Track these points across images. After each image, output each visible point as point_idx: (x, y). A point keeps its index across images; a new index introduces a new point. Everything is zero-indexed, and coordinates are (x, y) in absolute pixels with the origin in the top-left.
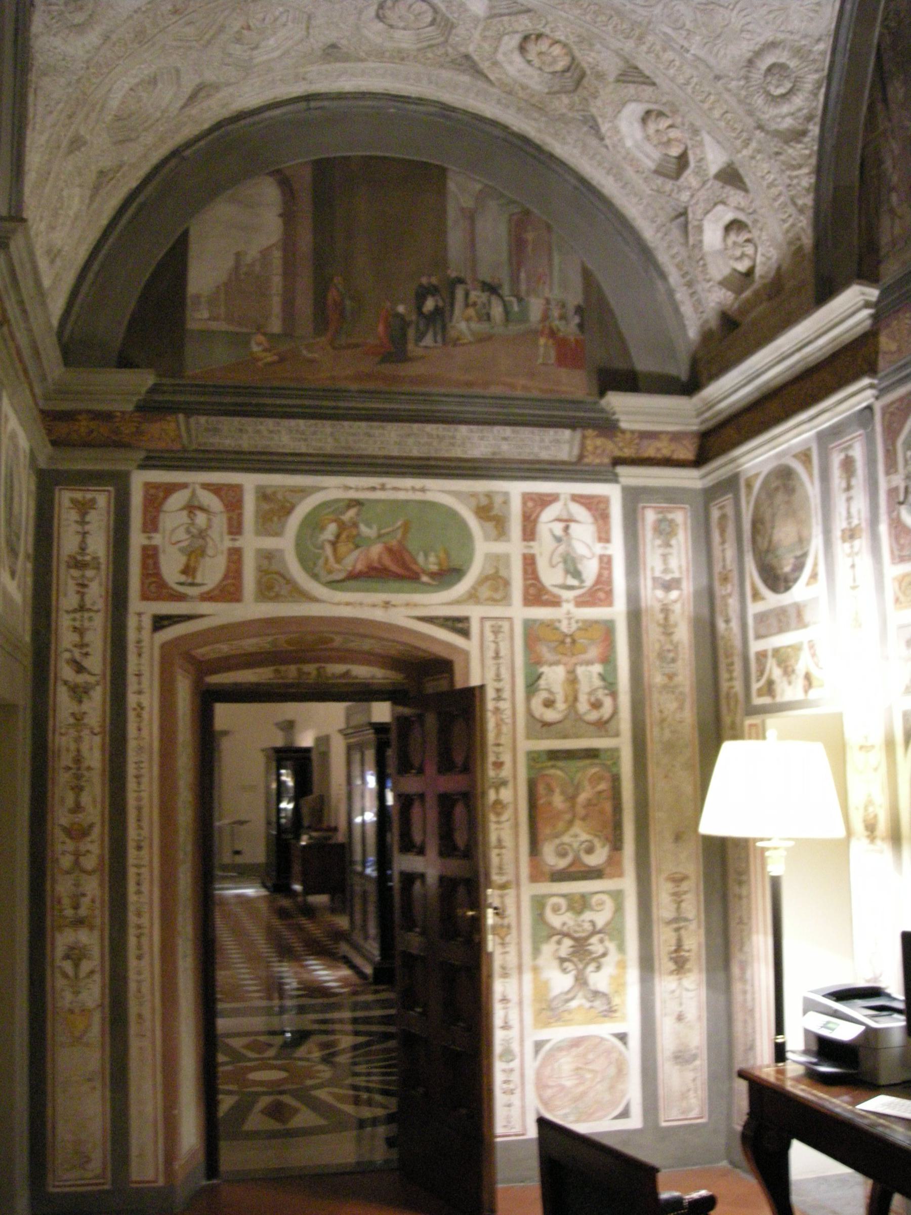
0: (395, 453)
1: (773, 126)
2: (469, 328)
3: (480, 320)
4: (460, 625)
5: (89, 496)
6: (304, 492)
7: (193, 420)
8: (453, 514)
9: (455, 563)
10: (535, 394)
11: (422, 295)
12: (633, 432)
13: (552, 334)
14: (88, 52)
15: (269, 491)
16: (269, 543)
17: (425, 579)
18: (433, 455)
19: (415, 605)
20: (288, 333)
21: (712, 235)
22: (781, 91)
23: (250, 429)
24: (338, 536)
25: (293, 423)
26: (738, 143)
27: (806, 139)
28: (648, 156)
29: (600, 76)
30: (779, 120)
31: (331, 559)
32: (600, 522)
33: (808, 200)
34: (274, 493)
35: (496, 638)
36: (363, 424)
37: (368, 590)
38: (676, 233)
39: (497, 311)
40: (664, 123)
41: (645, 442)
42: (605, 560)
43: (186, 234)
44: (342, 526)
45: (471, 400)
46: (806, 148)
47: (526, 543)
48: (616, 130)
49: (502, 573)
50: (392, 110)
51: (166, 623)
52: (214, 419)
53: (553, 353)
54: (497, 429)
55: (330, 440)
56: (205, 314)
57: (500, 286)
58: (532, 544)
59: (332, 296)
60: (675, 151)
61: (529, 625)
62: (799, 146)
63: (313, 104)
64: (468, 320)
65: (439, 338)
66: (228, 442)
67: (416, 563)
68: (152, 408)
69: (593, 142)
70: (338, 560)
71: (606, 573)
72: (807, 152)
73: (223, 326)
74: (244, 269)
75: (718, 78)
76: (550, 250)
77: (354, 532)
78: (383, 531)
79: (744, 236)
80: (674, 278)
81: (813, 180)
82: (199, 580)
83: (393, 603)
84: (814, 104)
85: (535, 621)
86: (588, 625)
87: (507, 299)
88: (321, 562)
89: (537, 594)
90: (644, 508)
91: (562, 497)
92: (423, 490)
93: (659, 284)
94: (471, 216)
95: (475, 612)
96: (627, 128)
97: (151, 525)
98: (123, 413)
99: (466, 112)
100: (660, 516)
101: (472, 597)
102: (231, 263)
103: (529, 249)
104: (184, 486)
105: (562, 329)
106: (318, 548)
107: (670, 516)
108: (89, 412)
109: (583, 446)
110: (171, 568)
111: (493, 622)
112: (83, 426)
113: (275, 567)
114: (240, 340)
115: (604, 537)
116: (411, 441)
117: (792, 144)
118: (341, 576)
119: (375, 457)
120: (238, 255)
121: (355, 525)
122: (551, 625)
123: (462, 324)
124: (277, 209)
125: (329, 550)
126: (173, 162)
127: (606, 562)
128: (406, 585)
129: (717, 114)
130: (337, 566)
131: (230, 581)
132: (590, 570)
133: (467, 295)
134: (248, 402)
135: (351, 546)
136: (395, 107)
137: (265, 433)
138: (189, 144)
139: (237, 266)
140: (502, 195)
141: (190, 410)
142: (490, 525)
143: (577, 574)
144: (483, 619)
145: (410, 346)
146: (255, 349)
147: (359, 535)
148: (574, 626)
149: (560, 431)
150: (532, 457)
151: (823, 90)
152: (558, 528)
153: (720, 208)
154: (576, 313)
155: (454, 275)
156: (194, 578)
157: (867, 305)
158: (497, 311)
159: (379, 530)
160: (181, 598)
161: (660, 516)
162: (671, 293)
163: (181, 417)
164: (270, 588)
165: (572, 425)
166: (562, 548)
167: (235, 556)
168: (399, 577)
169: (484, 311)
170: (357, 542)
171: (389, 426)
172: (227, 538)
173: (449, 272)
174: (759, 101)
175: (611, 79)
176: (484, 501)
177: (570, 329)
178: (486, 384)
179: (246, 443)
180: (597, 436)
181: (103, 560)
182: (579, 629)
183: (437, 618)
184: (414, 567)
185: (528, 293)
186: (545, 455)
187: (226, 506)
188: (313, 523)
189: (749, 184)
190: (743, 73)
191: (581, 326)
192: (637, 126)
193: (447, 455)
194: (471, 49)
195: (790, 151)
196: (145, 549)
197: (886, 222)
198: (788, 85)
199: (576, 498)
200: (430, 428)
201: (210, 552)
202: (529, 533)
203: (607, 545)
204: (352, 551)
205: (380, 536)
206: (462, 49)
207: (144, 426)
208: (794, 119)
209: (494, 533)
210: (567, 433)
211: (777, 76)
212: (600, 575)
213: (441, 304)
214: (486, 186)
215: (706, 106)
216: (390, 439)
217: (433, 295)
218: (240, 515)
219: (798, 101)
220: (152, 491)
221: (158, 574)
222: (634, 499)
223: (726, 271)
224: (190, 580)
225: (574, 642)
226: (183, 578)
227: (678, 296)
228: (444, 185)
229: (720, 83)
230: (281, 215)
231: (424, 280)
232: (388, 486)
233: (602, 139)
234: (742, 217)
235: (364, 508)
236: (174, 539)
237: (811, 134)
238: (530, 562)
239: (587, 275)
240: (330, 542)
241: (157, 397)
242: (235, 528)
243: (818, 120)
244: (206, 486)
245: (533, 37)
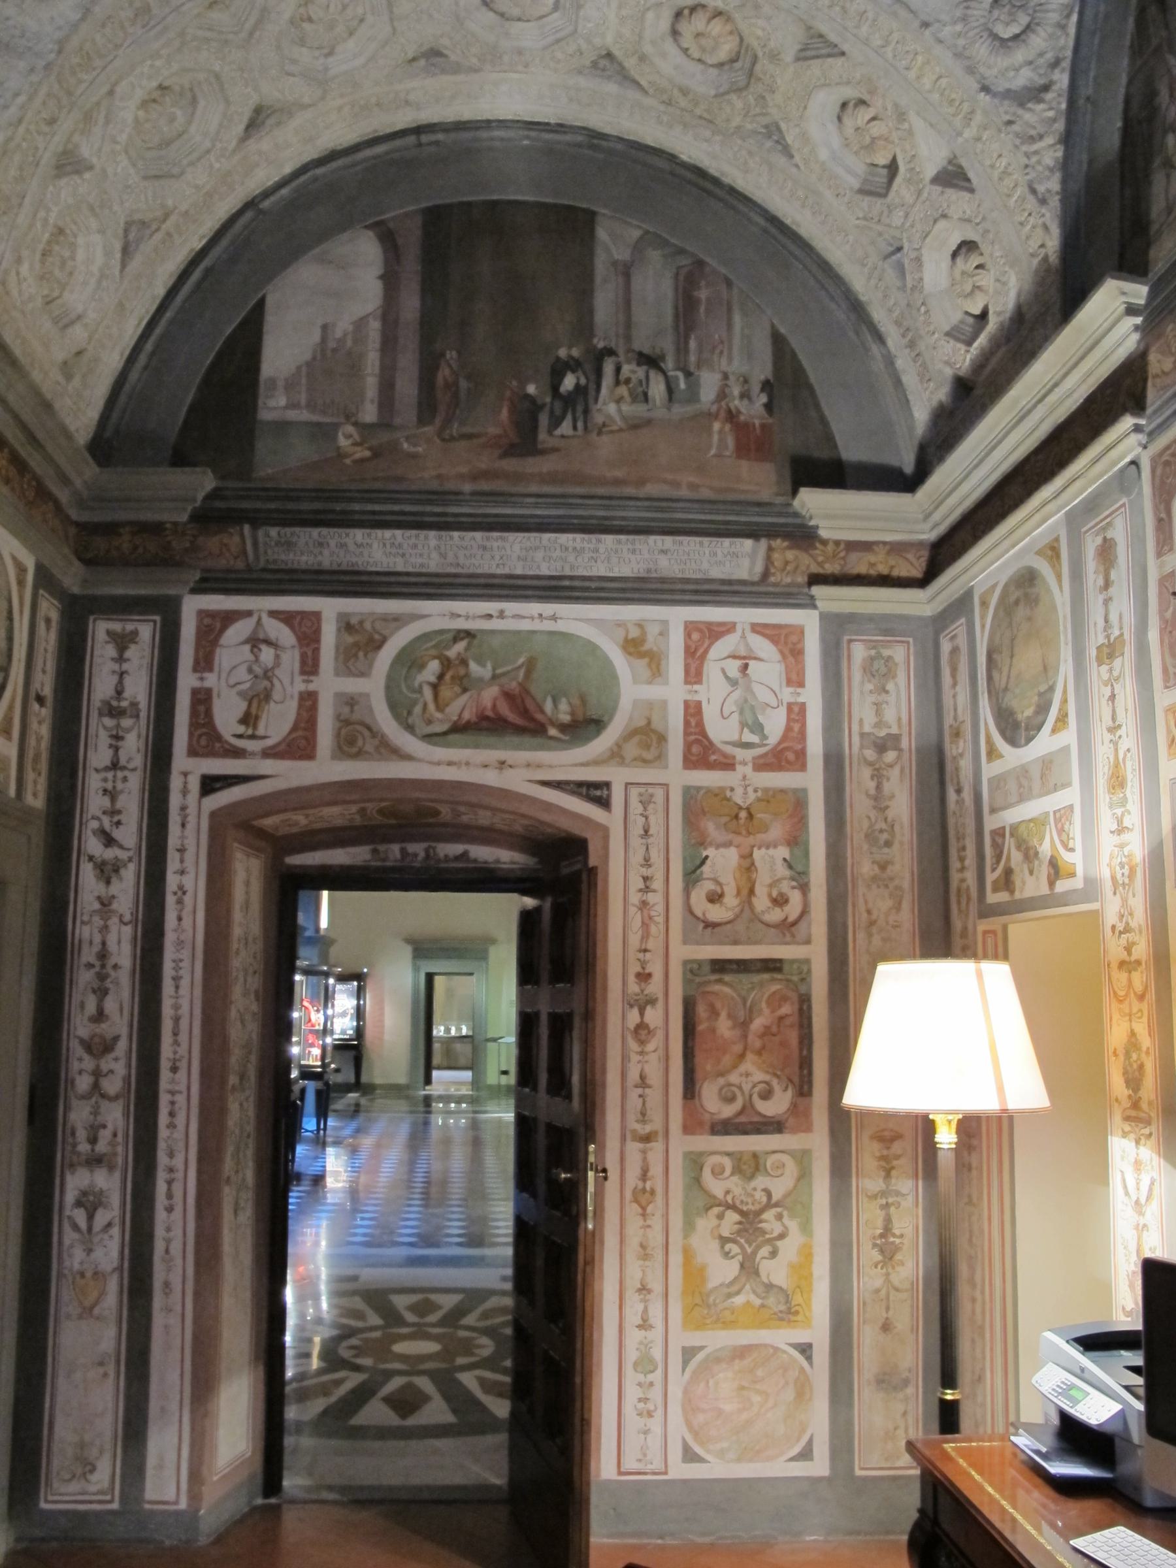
0: (519, 571)
1: (1002, 85)
2: (620, 411)
3: (634, 399)
4: (598, 793)
5: (130, 627)
6: (399, 621)
7: (261, 533)
8: (592, 648)
9: (593, 713)
10: (706, 493)
11: (558, 370)
12: (837, 543)
13: (731, 416)
14: (60, 28)
15: (354, 621)
16: (352, 685)
17: (552, 732)
18: (568, 572)
19: (539, 766)
20: (385, 423)
21: (936, 271)
22: (1015, 29)
23: (332, 543)
24: (441, 677)
25: (388, 533)
26: (958, 122)
27: (1049, 96)
29: (774, 57)
30: (1012, 74)
31: (431, 707)
32: (791, 659)
33: (1053, 184)
34: (361, 623)
35: (645, 809)
36: (478, 535)
37: (477, 747)
38: (891, 275)
39: (657, 389)
40: (864, 115)
41: (854, 556)
42: (796, 709)
43: (261, 303)
44: (446, 664)
45: (621, 503)
46: (1051, 109)
47: (689, 687)
48: (805, 137)
49: (656, 724)
50: (526, 142)
51: (218, 785)
52: (288, 530)
53: (730, 442)
54: (652, 539)
55: (434, 555)
56: (282, 401)
57: (662, 358)
58: (696, 687)
59: (444, 374)
60: (882, 159)
61: (690, 795)
62: (1042, 106)
63: (425, 138)
64: (619, 401)
65: (580, 424)
66: (304, 558)
67: (542, 712)
68: (211, 517)
69: (782, 161)
70: (439, 708)
71: (796, 727)
72: (1051, 114)
73: (304, 415)
74: (332, 344)
75: (926, 25)
76: (730, 310)
77: (462, 671)
78: (499, 671)
79: (975, 260)
80: (894, 340)
81: (1060, 154)
82: (261, 731)
83: (509, 762)
84: (1062, 41)
85: (698, 789)
86: (770, 797)
87: (671, 373)
88: (418, 709)
89: (701, 752)
90: (850, 641)
91: (739, 628)
92: (554, 618)
93: (875, 349)
94: (625, 271)
95: (617, 776)
96: (818, 131)
97: (204, 663)
98: (175, 524)
99: (620, 139)
100: (873, 652)
101: (616, 755)
102: (316, 336)
103: (702, 309)
104: (249, 614)
105: (743, 410)
106: (414, 691)
107: (886, 652)
108: (131, 523)
109: (769, 560)
110: (227, 716)
111: (642, 790)
112: (125, 542)
113: (356, 716)
114: (323, 432)
115: (796, 679)
116: (539, 555)
117: (1030, 105)
118: (445, 727)
119: (493, 576)
120: (325, 327)
121: (464, 662)
122: (720, 795)
123: (610, 406)
124: (377, 269)
125: (428, 693)
126: (249, 215)
127: (797, 713)
128: (527, 740)
129: (927, 82)
130: (438, 715)
131: (300, 733)
132: (775, 725)
133: (618, 369)
134: (331, 508)
135: (457, 689)
136: (528, 137)
137: (352, 547)
138: (266, 194)
139: (324, 340)
140: (666, 243)
141: (257, 520)
142: (642, 664)
143: (758, 728)
145: (542, 435)
146: (343, 442)
147: (467, 675)
148: (752, 796)
149: (738, 541)
150: (699, 576)
151: (1075, 18)
152: (733, 667)
153: (942, 224)
154: (762, 390)
155: (601, 345)
156: (255, 727)
157: (1131, 310)
158: (657, 389)
159: (494, 669)
160: (238, 753)
161: (873, 652)
162: (890, 361)
163: (247, 528)
164: (351, 742)
166: (737, 694)
167: (309, 702)
168: (520, 730)
169: (640, 390)
170: (465, 684)
171: (511, 536)
172: (298, 679)
173: (595, 341)
174: (982, 50)
175: (789, 56)
176: (634, 633)
177: (754, 410)
178: (641, 482)
179: (327, 559)
180: (789, 548)
181: (143, 706)
182: (759, 800)
183: (567, 783)
184: (539, 717)
185: (698, 367)
186: (716, 573)
187: (299, 639)
188: (409, 660)
189: (975, 181)
190: (958, 13)
191: (769, 407)
192: (832, 127)
193: (585, 573)
194: (609, 40)
195: (1027, 116)
196: (195, 692)
197: (1158, 181)
198: (1024, 19)
199: (757, 628)
200: (565, 538)
201: (277, 695)
202: (694, 675)
203: (799, 690)
204: (458, 696)
205: (494, 677)
206: (597, 41)
207: (201, 540)
208: (1034, 70)
209: (645, 673)
210: (748, 543)
211: (1006, 9)
212: (788, 729)
213: (583, 381)
214: (647, 232)
215: (912, 75)
216: (513, 553)
217: (573, 371)
218: (316, 651)
219: (1038, 41)
220: (207, 621)
221: (209, 723)
222: (837, 629)
223: (956, 317)
224: (250, 732)
225: (751, 816)
226: (241, 729)
227: (899, 363)
228: (592, 231)
229: (927, 32)
230: (381, 277)
231: (562, 353)
232: (507, 613)
233: (791, 157)
234: (971, 235)
235: (476, 642)
236: (232, 681)
237: (1055, 87)
238: (693, 712)
239: (779, 342)
240: (430, 684)
241: (219, 504)
242: (310, 666)
243: (1066, 64)
244: (273, 614)
245: (686, 12)
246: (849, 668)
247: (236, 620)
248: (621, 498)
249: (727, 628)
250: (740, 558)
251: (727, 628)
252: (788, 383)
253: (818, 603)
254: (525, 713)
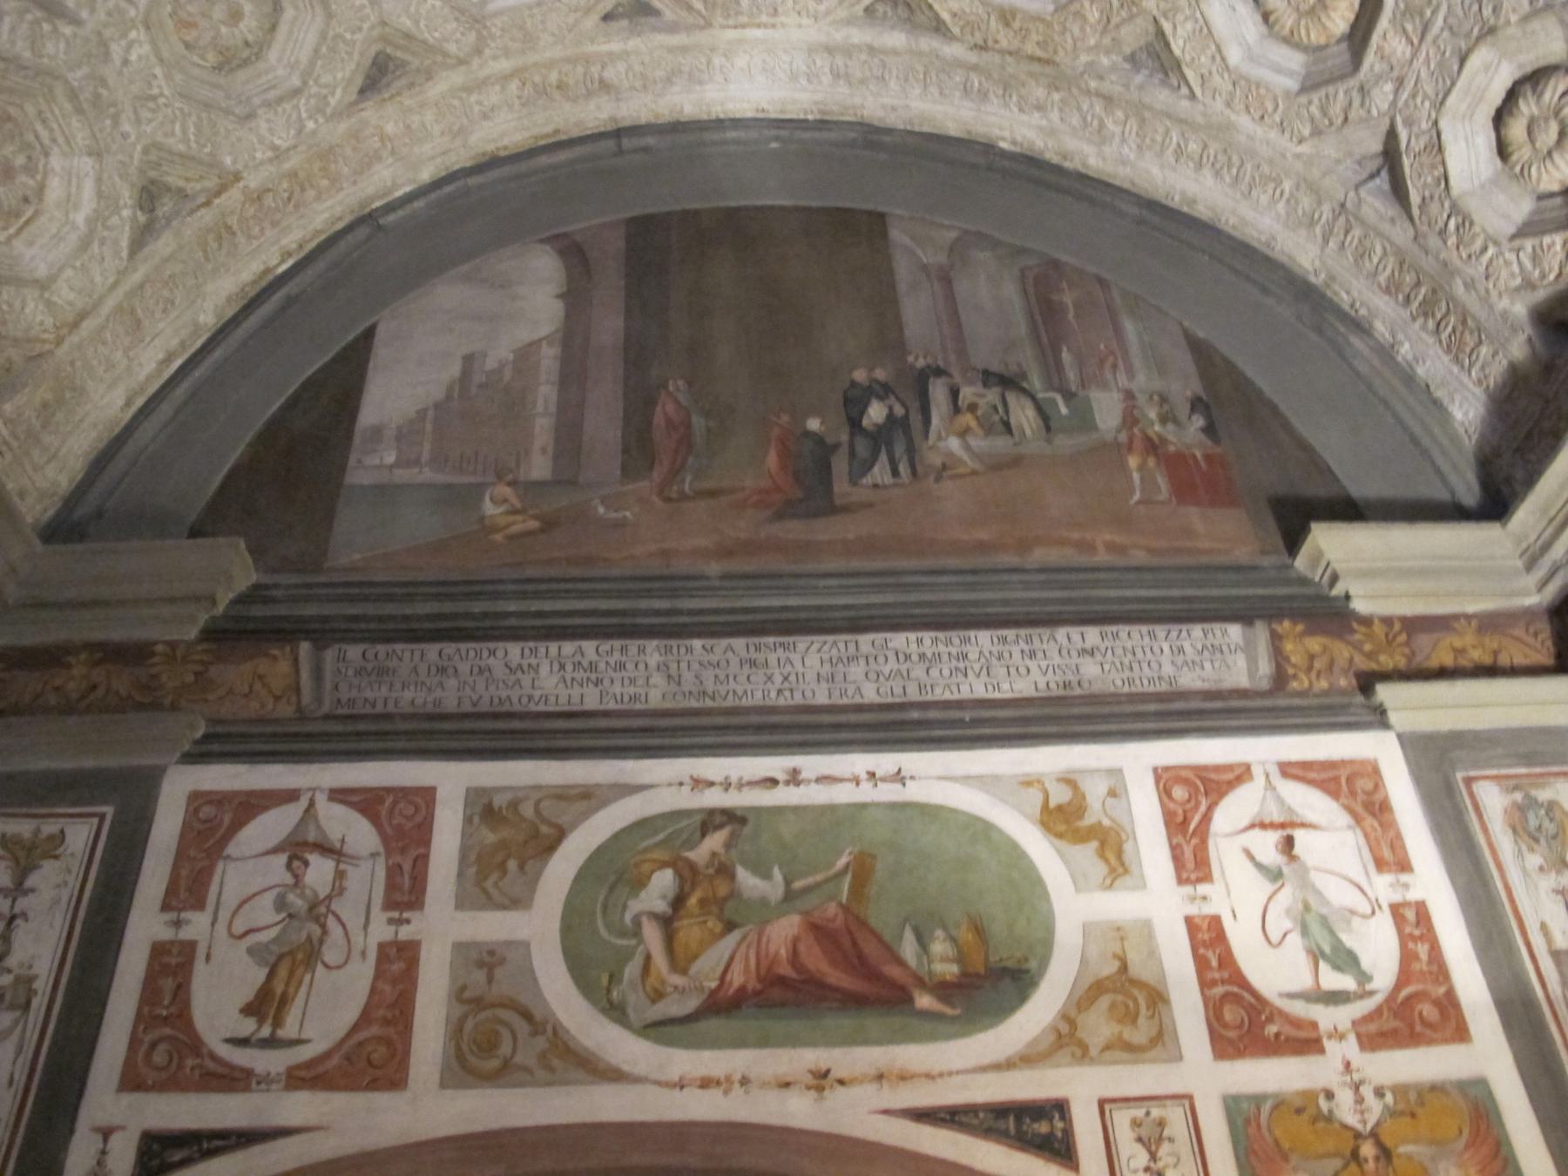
0: (822, 699)
2: (967, 448)
3: (989, 430)
4: (1043, 1128)
5: (50, 828)
6: (590, 798)
7: (330, 655)
8: (982, 830)
9: (1003, 954)
10: (1139, 557)
11: (854, 402)
12: (1387, 621)
13: (1153, 447)
15: (499, 801)
16: (492, 926)
17: (924, 1001)
18: (914, 695)
19: (904, 1077)
20: (566, 476)
23: (464, 668)
24: (678, 902)
25: (569, 647)
28: (1279, 70)
31: (660, 961)
32: (1370, 821)
34: (514, 805)
35: (1153, 1157)
36: (739, 643)
37: (764, 1042)
39: (1024, 415)
41: (1423, 640)
42: (1410, 915)
43: (369, 334)
44: (688, 875)
45: (995, 578)
47: (1188, 889)
49: (1137, 969)
50: (774, 145)
51: (178, 1156)
52: (381, 649)
53: (1162, 482)
54: (1061, 633)
55: (658, 679)
56: (390, 458)
58: (1203, 889)
59: (665, 409)
61: (1244, 1115)
63: (626, 143)
64: (964, 433)
65: (903, 468)
66: (408, 695)
67: (900, 962)
68: (237, 633)
70: (679, 964)
71: (1423, 950)
73: (427, 475)
74: (478, 378)
77: (723, 890)
78: (798, 884)
82: (289, 1030)
83: (837, 1073)
85: (1258, 1100)
86: (1414, 1102)
87: (1040, 395)
88: (632, 970)
89: (1244, 1022)
90: (1469, 781)
91: (1257, 771)
92: (899, 777)
95: (1080, 1087)
97: (188, 890)
98: (172, 645)
100: (1518, 796)
101: (1066, 1041)
102: (455, 369)
103: (1071, 315)
104: (291, 796)
105: (1171, 437)
106: (623, 934)
107: (1543, 795)
108: (90, 647)
109: (1278, 655)
110: (217, 1006)
111: (1139, 1113)
112: (74, 678)
113: (504, 985)
115: (1391, 858)
116: (857, 671)
118: (692, 1004)
119: (773, 710)
120: (468, 360)
121: (725, 871)
122: (1307, 1109)
123: (949, 442)
125: (652, 935)
126: (362, 232)
127: (1414, 923)
128: (873, 1022)
130: (677, 980)
131: (375, 1030)
132: (1379, 950)
133: (954, 393)
135: (713, 924)
136: (777, 138)
137: (499, 671)
139: (466, 374)
140: (996, 244)
141: (323, 634)
142: (1086, 853)
143: (1346, 960)
144: (1104, 1105)
145: (841, 486)
146: (489, 509)
147: (734, 894)
148: (1375, 1108)
149: (1217, 627)
150: (1163, 687)
152: (1266, 845)
154: (1193, 409)
155: (921, 363)
156: (278, 1023)
158: (1024, 415)
159: (788, 882)
160: (233, 1080)
161: (1518, 796)
163: (305, 647)
164: (488, 1045)
165: (1244, 616)
166: (1286, 897)
167: (399, 964)
168: (854, 1002)
169: (996, 418)
170: (729, 913)
171: (802, 642)
172: (379, 917)
173: (911, 359)
176: (1060, 795)
177: (1189, 434)
178: (1024, 546)
179: (450, 697)
180: (1310, 632)
181: (42, 985)
182: (1391, 1113)
183: (972, 1109)
184: (892, 971)
185: (1083, 384)
186: (1190, 680)
187: (385, 840)
188: (612, 871)
191: (1210, 430)
193: (947, 696)
196: (158, 950)
199: (1291, 770)
200: (899, 640)
201: (331, 954)
202: (1192, 863)
203: (1404, 878)
204: (718, 937)
205: (790, 896)
207: (213, 671)
209: (1099, 870)
210: (1235, 631)
212: (1407, 958)
213: (899, 411)
214: (966, 232)
216: (808, 670)
217: (881, 398)
218: (422, 862)
220: (207, 812)
221: (182, 1016)
222: (1437, 760)
224: (266, 1032)
225: (1385, 1153)
226: (248, 1026)
228: (884, 235)
230: (560, 296)
231: (860, 375)
232: (804, 775)
235: (747, 830)
236: (238, 928)
238: (1208, 938)
239: (1200, 350)
240: (654, 916)
241: (257, 611)
242: (406, 892)
244: (340, 795)
246: (1485, 830)
247: (265, 808)
248: (996, 571)
249: (1240, 774)
250: (1229, 656)
251: (1240, 774)
252: (1225, 396)
253: (1393, 717)
254: (862, 966)
